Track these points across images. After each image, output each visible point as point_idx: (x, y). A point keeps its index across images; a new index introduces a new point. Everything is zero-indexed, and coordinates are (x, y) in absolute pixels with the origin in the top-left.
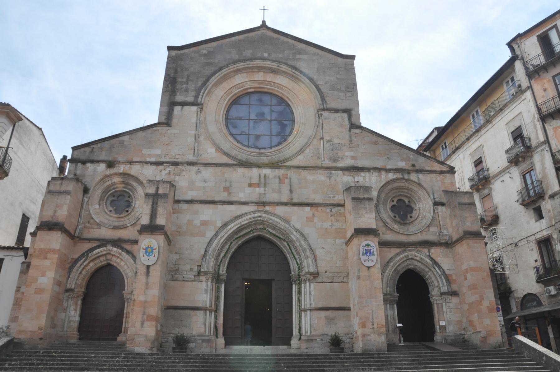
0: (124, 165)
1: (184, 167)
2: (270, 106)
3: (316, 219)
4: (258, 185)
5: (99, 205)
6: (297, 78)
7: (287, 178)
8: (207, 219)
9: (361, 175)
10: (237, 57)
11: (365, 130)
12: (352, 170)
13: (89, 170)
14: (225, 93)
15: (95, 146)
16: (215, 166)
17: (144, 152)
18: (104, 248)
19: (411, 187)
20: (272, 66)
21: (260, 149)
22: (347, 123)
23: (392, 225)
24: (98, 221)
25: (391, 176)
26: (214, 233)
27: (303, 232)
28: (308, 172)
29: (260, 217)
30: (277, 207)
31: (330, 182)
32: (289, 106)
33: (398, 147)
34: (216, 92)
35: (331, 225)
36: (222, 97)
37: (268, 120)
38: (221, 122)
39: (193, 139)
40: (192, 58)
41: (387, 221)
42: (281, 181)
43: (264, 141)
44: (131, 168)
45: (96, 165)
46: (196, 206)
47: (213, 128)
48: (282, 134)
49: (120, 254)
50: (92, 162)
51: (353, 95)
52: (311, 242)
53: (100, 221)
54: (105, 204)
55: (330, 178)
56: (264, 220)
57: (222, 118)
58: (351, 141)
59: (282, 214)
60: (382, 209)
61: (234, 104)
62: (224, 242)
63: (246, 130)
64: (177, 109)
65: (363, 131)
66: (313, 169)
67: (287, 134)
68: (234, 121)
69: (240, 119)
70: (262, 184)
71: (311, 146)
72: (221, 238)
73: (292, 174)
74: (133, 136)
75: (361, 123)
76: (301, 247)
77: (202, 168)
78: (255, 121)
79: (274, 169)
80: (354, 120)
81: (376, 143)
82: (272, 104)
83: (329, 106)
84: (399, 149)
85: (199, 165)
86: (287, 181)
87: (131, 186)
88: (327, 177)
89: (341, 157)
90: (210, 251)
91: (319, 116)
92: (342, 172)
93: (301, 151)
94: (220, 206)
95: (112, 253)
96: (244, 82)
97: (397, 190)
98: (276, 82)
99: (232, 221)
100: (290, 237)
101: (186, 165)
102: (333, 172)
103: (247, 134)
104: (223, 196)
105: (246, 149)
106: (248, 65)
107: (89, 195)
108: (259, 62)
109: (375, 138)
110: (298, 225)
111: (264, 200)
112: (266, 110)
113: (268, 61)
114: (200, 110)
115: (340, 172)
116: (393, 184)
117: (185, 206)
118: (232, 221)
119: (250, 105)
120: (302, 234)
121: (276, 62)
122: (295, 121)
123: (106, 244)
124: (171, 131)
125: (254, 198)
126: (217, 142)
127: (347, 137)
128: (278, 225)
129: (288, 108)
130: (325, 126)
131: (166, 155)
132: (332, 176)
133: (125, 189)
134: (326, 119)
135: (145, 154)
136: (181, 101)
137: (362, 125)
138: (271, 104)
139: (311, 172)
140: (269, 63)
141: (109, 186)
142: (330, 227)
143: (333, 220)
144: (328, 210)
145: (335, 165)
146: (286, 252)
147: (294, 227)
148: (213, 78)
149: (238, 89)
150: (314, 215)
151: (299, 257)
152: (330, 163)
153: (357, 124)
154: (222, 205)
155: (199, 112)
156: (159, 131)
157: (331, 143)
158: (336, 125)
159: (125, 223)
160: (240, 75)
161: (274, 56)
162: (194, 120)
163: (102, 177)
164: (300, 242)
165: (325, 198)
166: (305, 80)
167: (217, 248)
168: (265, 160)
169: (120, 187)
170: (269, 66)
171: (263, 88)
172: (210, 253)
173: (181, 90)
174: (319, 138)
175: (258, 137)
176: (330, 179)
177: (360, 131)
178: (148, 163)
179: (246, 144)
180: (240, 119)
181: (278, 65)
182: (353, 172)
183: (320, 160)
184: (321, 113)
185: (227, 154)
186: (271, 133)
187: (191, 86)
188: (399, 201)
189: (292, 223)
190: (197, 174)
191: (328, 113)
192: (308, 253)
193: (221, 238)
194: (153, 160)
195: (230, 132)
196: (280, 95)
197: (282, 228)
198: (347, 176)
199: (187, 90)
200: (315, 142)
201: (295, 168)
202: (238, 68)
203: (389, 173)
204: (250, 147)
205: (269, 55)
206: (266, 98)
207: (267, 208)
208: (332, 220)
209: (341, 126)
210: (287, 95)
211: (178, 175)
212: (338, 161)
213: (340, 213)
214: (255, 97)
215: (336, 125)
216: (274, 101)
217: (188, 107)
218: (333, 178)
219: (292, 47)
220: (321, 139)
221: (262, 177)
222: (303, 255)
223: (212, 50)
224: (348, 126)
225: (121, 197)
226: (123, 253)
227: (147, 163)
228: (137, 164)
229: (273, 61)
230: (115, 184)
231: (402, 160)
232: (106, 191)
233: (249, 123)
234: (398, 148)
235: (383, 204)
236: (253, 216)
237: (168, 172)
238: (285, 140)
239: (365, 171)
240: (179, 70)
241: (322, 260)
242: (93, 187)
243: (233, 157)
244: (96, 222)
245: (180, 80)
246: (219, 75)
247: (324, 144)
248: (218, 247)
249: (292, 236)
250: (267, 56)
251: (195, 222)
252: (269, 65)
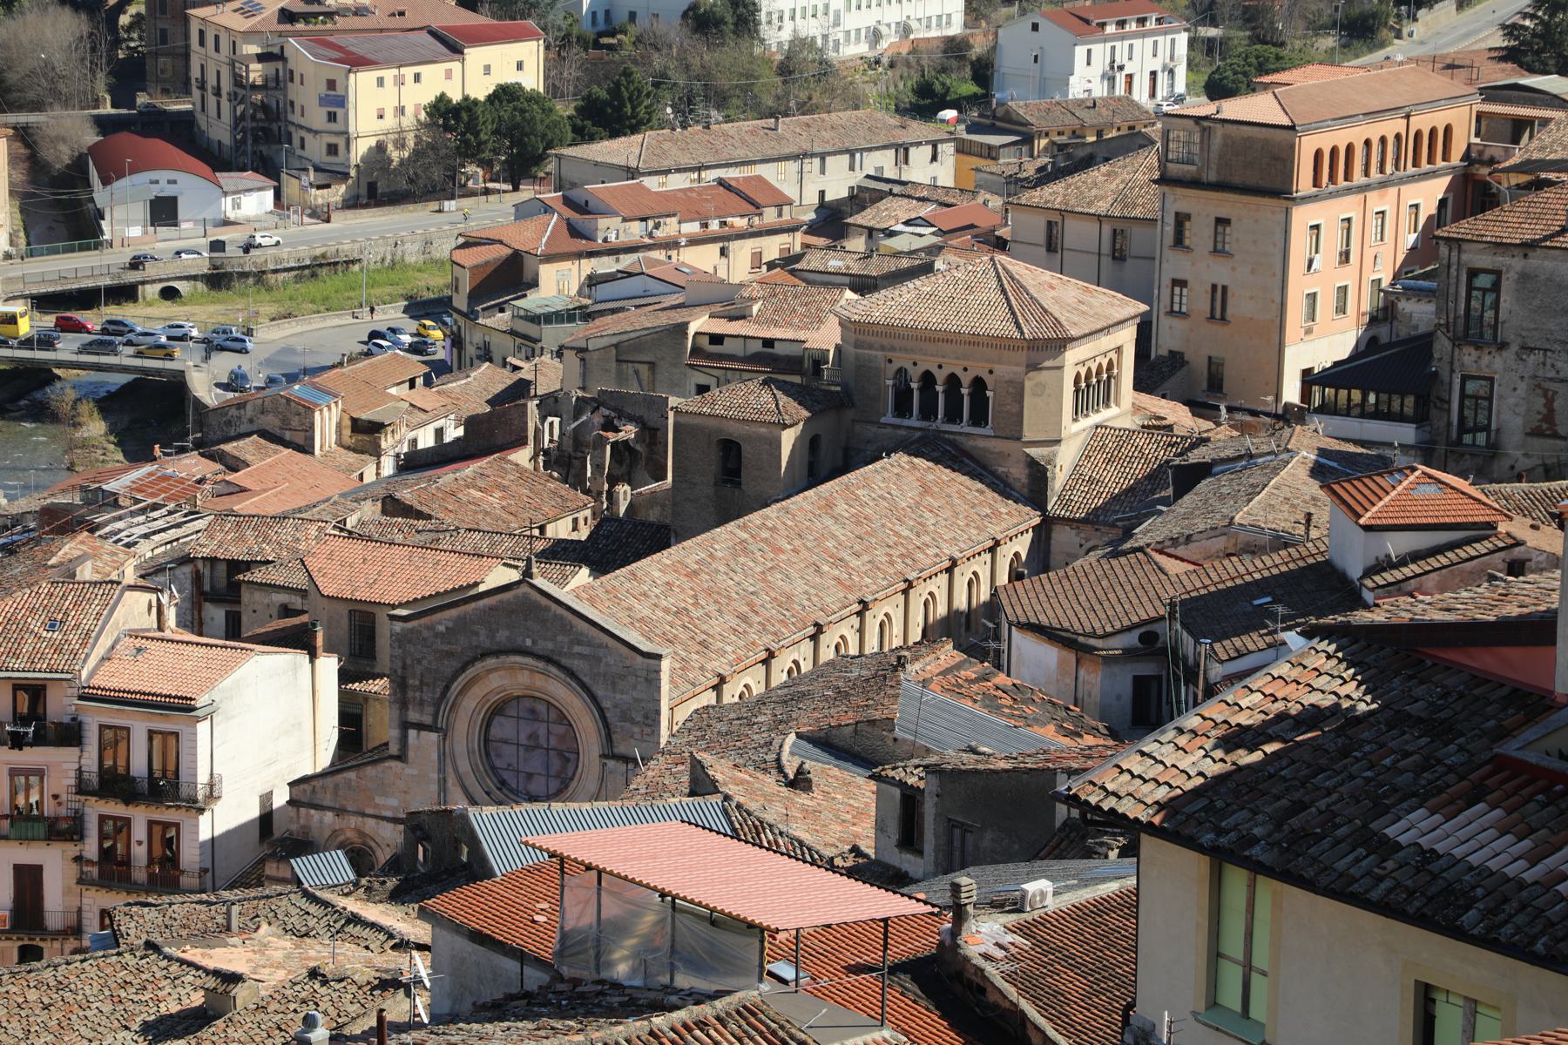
10: (487, 644)
17: (378, 800)
40: (424, 639)
47: (464, 766)
51: (653, 732)
67: (570, 775)
69: (506, 742)
78: (529, 749)
126: (470, 790)
162: (435, 756)
175: (530, 776)
180: (506, 742)
187: (427, 696)
194: (389, 814)
199: (422, 703)
205: (534, 642)
216: (553, 715)
223: (451, 625)
238: (567, 787)
240: (408, 662)
245: (411, 682)
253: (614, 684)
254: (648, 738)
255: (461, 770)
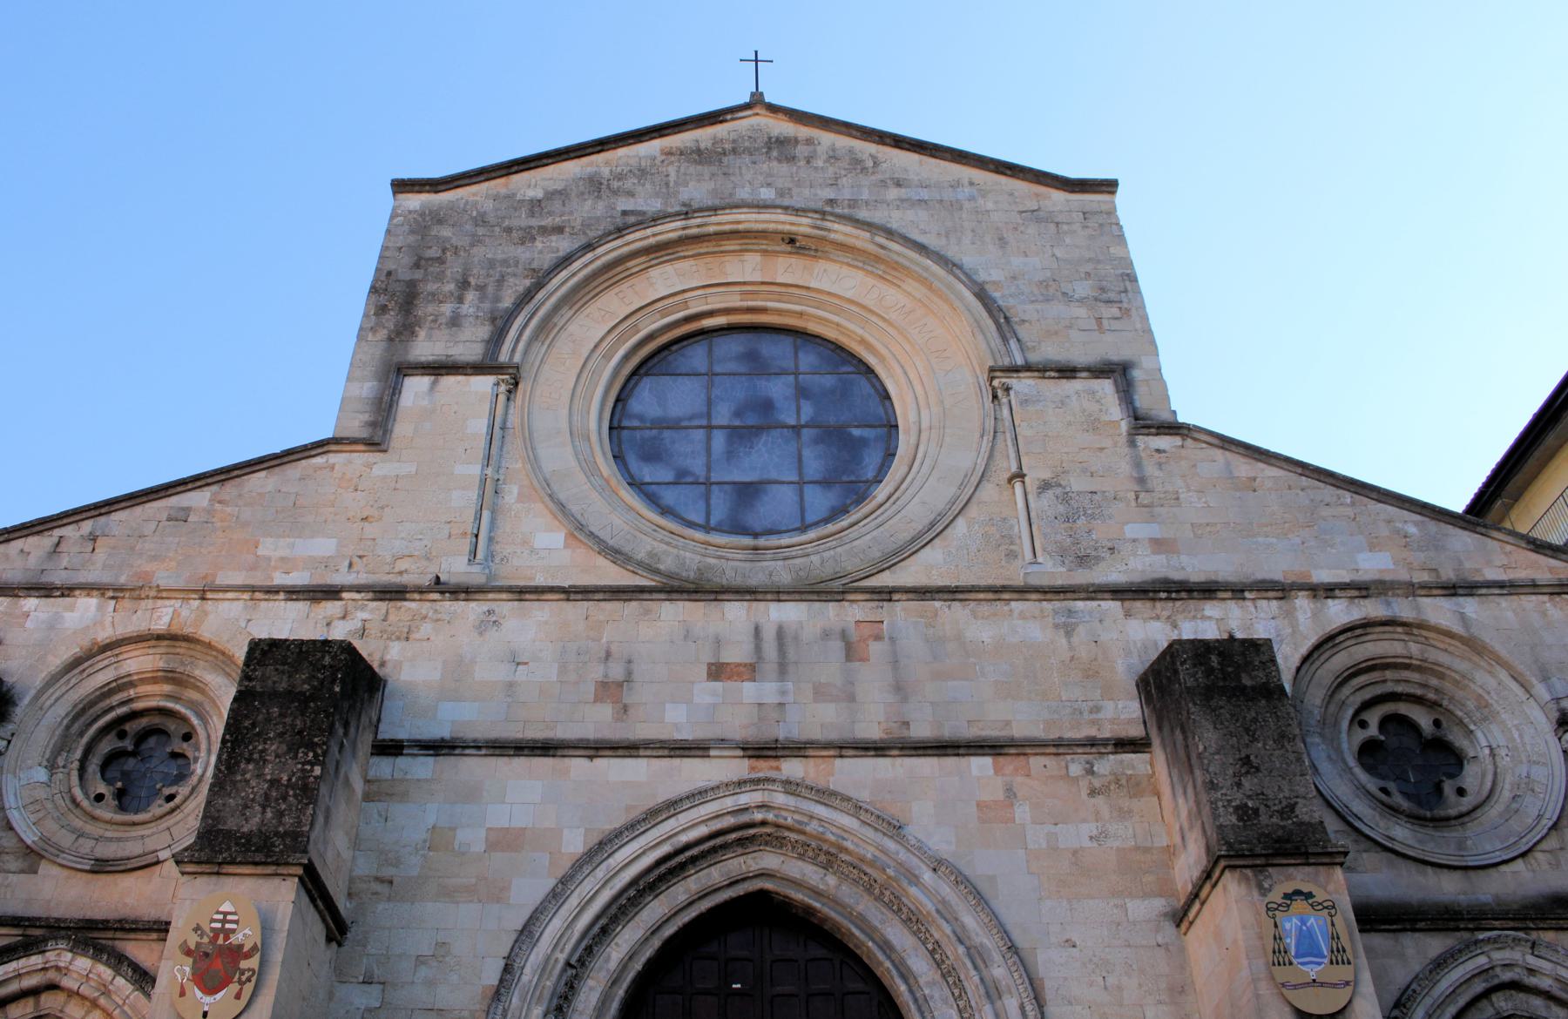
0: (178, 604)
1: (428, 604)
2: (791, 378)
3: (1022, 812)
4: (750, 671)
5: (52, 767)
6: (896, 266)
7: (878, 638)
8: (518, 823)
9: (1208, 612)
11: (1195, 439)
12: (1163, 595)
13: (29, 624)
14: (609, 332)
15: (68, 531)
16: (562, 596)
18: (35, 961)
19: (1433, 655)
20: (794, 229)
21: (756, 535)
22: (1115, 412)
23: (1382, 824)
24: (30, 838)
25: (1339, 612)
26: (550, 883)
27: (967, 872)
28: (967, 611)
29: (762, 806)
30: (838, 761)
31: (1071, 648)
32: (869, 371)
33: (1347, 497)
34: (572, 328)
35: (1095, 832)
36: (596, 347)
37: (788, 427)
38: (594, 438)
39: (474, 494)
41: (1355, 810)
42: (851, 651)
43: (778, 504)
44: (206, 614)
45: (56, 604)
46: (472, 767)
47: (558, 456)
48: (853, 478)
49: (106, 992)
50: (45, 590)
51: (1126, 313)
52: (1010, 917)
53: (44, 839)
54: (76, 765)
55: (1069, 630)
56: (781, 821)
57: (594, 419)
58: (1141, 480)
59: (864, 795)
60: (1323, 755)
61: (647, 374)
62: (596, 929)
63: (697, 466)
64: (415, 387)
65: (1189, 442)
66: (990, 596)
67: (870, 475)
68: (648, 433)
69: (675, 425)
70: (770, 667)
71: (973, 511)
72: (583, 909)
73: (901, 614)
74: (230, 490)
75: (1174, 412)
76: (961, 941)
77: (506, 608)
79: (817, 604)
80: (1142, 401)
81: (1251, 485)
82: (803, 367)
83: (1034, 358)
84: (1353, 504)
85: (491, 596)
86: (875, 648)
87: (197, 688)
88: (1056, 626)
89: (1110, 545)
90: (527, 970)
91: (995, 397)
92: (1118, 603)
93: (933, 531)
94: (578, 766)
95: (67, 982)
96: (684, 291)
97: (1375, 676)
98: (811, 286)
99: (633, 828)
100: (908, 897)
101: (436, 596)
102: (1080, 604)
103: (701, 480)
104: (597, 722)
105: (699, 535)
106: (698, 226)
107: (11, 727)
108: (742, 217)
109: (1244, 468)
110: (941, 842)
111: (781, 733)
112: (778, 389)
113: (779, 211)
114: (509, 391)
115: (1112, 606)
116: (1353, 649)
117: (421, 767)
118: (633, 828)
119: (711, 374)
120: (961, 880)
121: (810, 215)
122: (897, 426)
123: (45, 940)
124: (381, 467)
125: (738, 725)
126: (574, 508)
127: (1125, 468)
128: (848, 844)
129: (867, 379)
130: (1024, 431)
131: (356, 560)
132: (1077, 624)
133: (170, 705)
134: (1025, 402)
135: (269, 559)
136: (431, 358)
137: (1181, 419)
138: (797, 367)
139: (985, 608)
140: (783, 218)
141: (107, 691)
142: (1095, 844)
143: (1105, 812)
144: (1076, 769)
145: (1082, 577)
146: (894, 972)
147: (920, 850)
148: (564, 274)
149: (663, 318)
150: (1010, 792)
151: (956, 992)
152: (1063, 569)
153: (1165, 416)
154: (591, 757)
155: (502, 398)
156: (337, 467)
157: (1059, 491)
158: (1070, 424)
159: (151, 845)
160: (668, 268)
161: (800, 198)
162: (480, 426)
163: (78, 650)
164: (953, 919)
165: (1056, 716)
166: (926, 269)
167: (562, 957)
168: (781, 572)
169: (151, 696)
170: (780, 227)
171: (763, 310)
172: (525, 979)
173: (435, 321)
174: (1007, 475)
175: (748, 492)
176: (1068, 634)
177: (1177, 441)
178: (277, 592)
179: (698, 518)
181: (819, 222)
182: (1170, 604)
183: (1018, 563)
184: (1004, 380)
185: (616, 555)
186: (800, 474)
188: (1384, 723)
189: (912, 831)
190: (481, 634)
191: (1031, 382)
192: (998, 971)
193: (583, 909)
195: (632, 477)
196: (831, 334)
197: (869, 856)
198: (1145, 620)
199: (455, 321)
200: (988, 492)
201: (911, 596)
202: (659, 238)
203: (1330, 601)
204: (713, 529)
206: (776, 350)
207: (792, 768)
208: (1097, 813)
209: (1094, 425)
210: (860, 331)
211: (398, 638)
212: (1098, 559)
213: (1129, 778)
214: (732, 346)
215: (1070, 424)
217: (460, 378)
218: (1081, 633)
219: (870, 164)
220: (1010, 480)
221: (769, 635)
222: (976, 979)
224: (1124, 426)
225: (152, 741)
226: (120, 981)
227: (272, 591)
228: (230, 595)
229: (797, 211)
230: (132, 684)
231: (1372, 547)
232: (82, 711)
233: (709, 439)
234: (1349, 501)
235: (1321, 735)
236: (729, 803)
237: (360, 624)
238: (861, 499)
239: (1221, 595)
241: (1070, 1003)
242: (33, 692)
243: (640, 564)
244: (21, 840)
246: (586, 266)
247: (1030, 497)
248: (569, 947)
249: (913, 890)
250: (773, 197)
251: (463, 836)
252: (783, 223)
253: (1002, 242)
254: (1116, 325)
255: (548, 466)
